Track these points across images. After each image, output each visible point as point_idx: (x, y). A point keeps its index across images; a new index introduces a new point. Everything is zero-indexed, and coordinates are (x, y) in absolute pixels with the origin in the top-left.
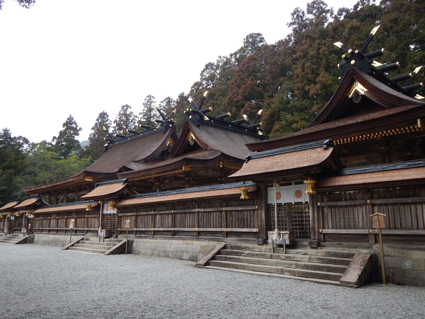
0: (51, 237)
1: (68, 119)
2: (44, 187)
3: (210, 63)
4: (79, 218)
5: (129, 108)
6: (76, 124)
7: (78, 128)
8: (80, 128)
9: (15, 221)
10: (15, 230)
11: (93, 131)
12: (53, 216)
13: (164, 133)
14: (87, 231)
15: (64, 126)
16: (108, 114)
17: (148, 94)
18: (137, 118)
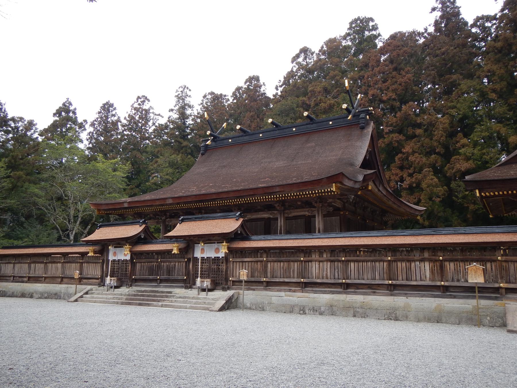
0: (324, 298)
1: (64, 104)
2: (170, 201)
3: (305, 47)
4: (450, 261)
5: (147, 102)
6: (74, 113)
7: (80, 120)
8: (85, 121)
9: (133, 264)
10: (136, 280)
11: (91, 129)
12: (313, 256)
13: (363, 128)
14: (506, 289)
15: (54, 115)
16: (115, 106)
17: (182, 84)
18: (160, 118)
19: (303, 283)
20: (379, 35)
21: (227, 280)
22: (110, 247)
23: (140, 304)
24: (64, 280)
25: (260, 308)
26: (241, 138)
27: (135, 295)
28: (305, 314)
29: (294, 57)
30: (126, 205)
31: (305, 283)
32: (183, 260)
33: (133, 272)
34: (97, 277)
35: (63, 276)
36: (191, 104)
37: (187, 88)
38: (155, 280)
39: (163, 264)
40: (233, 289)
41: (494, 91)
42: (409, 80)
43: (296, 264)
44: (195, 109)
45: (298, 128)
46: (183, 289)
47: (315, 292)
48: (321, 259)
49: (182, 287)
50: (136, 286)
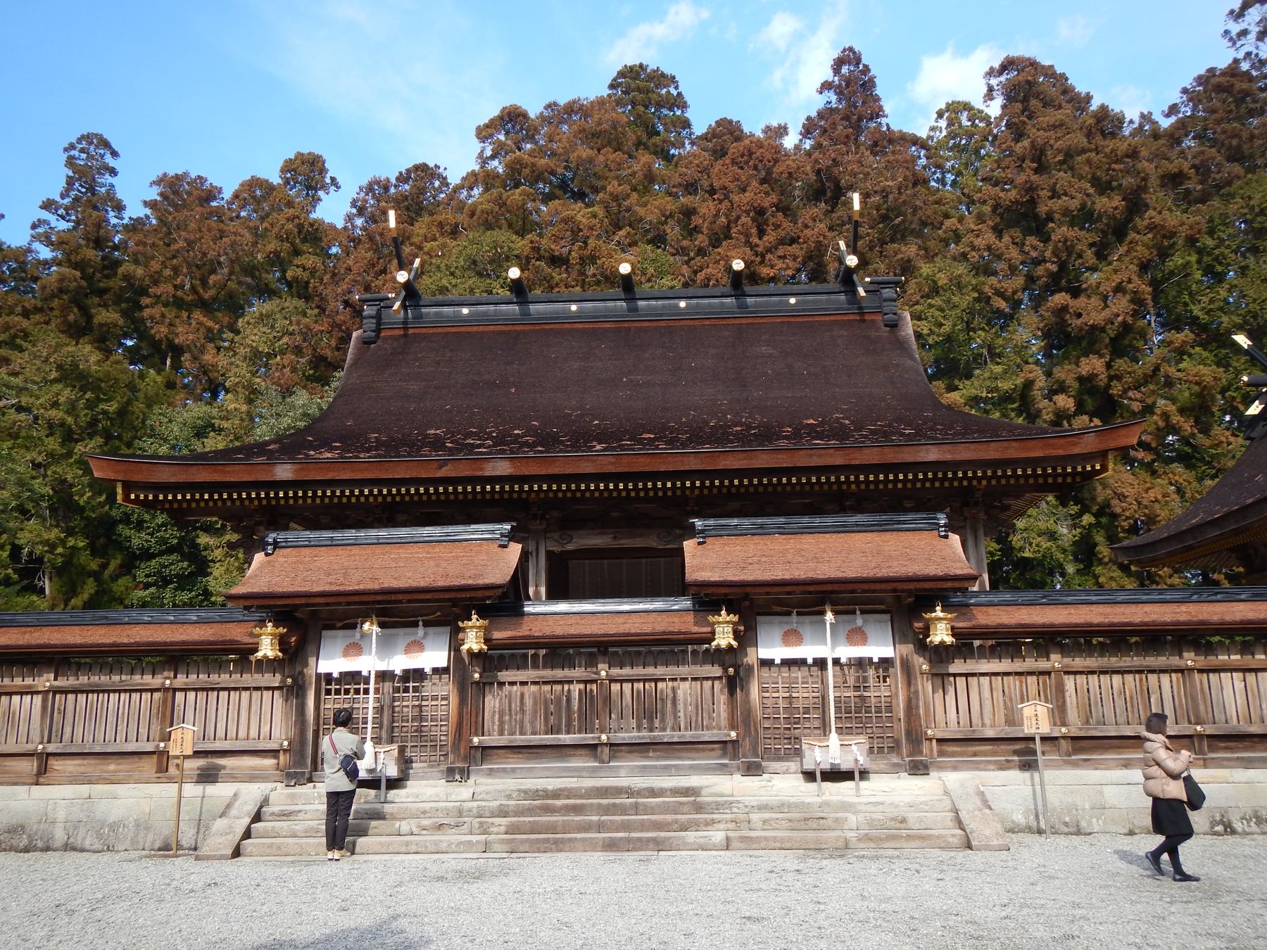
2: (502, 468)
10: (486, 751)
19: (1201, 736)
20: (686, 124)
21: (915, 737)
22: (366, 626)
23: (611, 846)
24: (55, 764)
25: (1066, 824)
26: (504, 307)
27: (530, 811)
28: (1233, 832)
29: (487, 126)
30: (284, 472)
31: (1209, 736)
32: (716, 671)
33: (469, 718)
34: (275, 746)
35: (51, 748)
36: (119, 195)
37: (106, 144)
38: (592, 749)
39: (615, 687)
40: (941, 767)
41: (1000, 294)
42: (825, 237)
43: (1165, 679)
44: (127, 214)
45: (694, 301)
46: (737, 777)
47: (1248, 764)
48: (1248, 660)
49: (723, 769)
50: (491, 772)
